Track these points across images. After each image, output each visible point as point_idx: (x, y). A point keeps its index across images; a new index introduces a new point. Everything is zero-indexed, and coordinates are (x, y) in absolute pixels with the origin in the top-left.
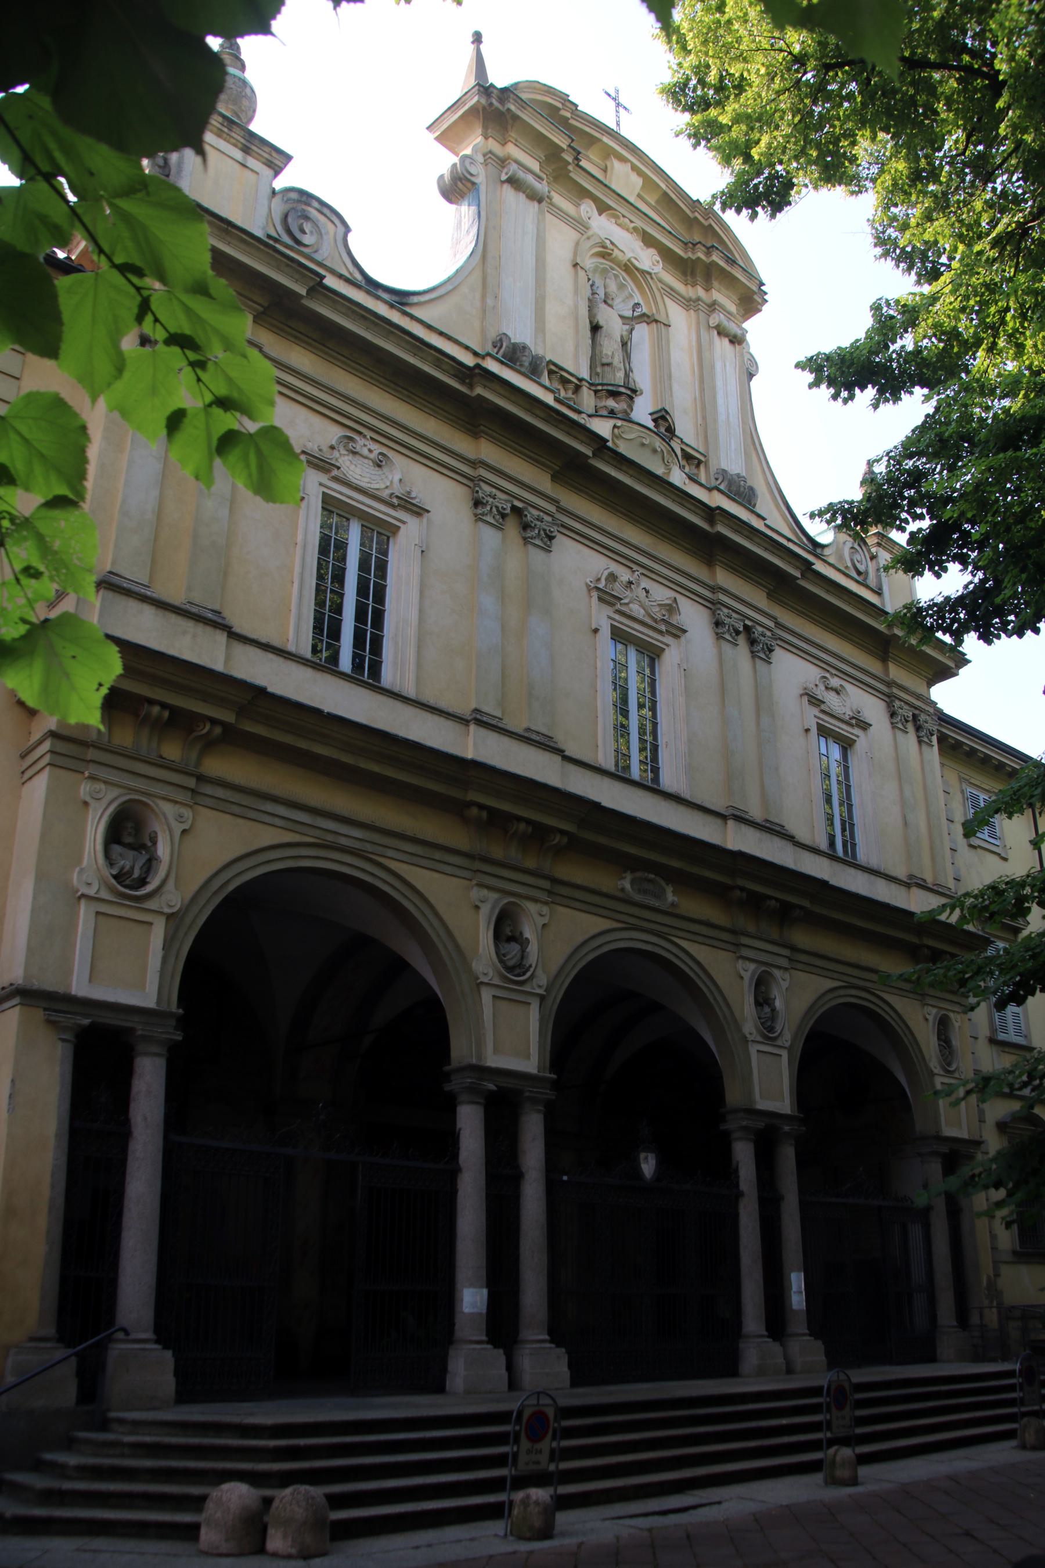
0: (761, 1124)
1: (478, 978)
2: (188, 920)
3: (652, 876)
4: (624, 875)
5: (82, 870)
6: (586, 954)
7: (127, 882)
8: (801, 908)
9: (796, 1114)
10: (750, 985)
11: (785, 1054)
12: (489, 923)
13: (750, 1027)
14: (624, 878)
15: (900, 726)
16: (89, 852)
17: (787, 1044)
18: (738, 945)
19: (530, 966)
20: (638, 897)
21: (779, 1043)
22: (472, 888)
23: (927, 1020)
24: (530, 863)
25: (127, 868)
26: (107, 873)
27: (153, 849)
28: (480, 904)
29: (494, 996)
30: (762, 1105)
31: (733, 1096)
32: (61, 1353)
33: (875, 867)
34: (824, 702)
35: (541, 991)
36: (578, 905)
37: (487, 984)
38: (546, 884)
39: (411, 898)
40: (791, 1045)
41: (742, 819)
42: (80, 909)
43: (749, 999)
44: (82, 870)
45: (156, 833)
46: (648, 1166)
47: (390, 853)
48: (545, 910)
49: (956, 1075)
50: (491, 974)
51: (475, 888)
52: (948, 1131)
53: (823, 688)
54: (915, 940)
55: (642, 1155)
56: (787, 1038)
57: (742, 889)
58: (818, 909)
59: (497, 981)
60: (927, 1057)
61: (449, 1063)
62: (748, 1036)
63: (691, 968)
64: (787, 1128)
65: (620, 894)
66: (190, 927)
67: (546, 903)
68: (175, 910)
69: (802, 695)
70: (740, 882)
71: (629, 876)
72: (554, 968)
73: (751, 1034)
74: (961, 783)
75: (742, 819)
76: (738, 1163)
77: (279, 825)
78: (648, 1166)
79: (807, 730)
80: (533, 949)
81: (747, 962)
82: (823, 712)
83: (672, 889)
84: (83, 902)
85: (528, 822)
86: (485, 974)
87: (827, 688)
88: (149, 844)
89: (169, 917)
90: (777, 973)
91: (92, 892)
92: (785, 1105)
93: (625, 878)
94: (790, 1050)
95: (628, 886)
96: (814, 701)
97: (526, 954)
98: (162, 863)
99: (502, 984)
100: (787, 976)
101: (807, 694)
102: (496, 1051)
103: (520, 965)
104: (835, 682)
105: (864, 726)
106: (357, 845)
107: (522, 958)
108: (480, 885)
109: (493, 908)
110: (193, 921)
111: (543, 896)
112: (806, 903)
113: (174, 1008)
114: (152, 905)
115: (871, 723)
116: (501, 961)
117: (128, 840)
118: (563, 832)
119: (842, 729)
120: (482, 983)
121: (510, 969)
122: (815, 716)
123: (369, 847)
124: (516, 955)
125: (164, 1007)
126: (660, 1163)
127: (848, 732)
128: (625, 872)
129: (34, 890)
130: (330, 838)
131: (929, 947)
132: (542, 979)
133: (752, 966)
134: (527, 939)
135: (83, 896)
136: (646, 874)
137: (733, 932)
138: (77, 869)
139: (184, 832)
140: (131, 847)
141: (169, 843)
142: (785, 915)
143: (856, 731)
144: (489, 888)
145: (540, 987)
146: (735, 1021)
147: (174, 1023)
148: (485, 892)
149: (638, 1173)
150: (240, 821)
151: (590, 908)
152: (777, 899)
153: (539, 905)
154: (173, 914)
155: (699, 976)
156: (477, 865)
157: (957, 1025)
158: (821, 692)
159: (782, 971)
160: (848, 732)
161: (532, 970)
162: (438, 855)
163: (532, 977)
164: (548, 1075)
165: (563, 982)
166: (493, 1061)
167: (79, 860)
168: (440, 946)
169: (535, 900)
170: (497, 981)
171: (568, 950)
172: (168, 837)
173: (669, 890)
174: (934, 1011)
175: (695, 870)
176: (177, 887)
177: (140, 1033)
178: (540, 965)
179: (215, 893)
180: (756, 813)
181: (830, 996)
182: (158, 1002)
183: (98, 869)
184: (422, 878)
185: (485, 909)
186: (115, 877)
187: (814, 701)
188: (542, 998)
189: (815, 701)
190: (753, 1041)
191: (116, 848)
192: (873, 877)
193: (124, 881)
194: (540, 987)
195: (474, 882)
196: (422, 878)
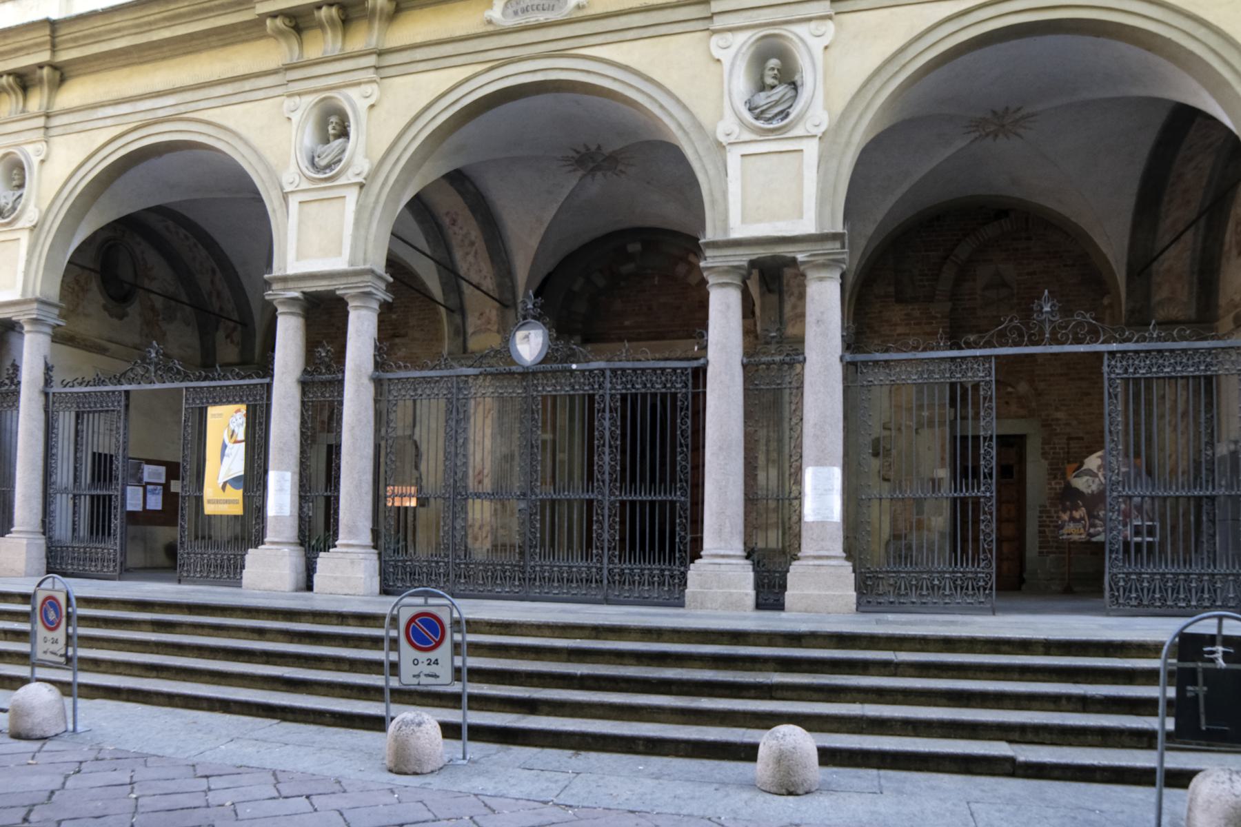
2: (46, 227)
18: (710, 18)
28: (291, 115)
35: (360, 179)
37: (292, 192)
38: (372, 60)
59: (305, 185)
63: (615, 79)
65: (490, 28)
66: (49, 231)
77: (110, 124)
81: (729, 35)
102: (300, 256)
108: (290, 95)
110: (51, 227)
111: (370, 74)
114: (19, 225)
123: (182, 109)
130: (150, 116)
139: (43, 161)
146: (700, 127)
148: (297, 99)
150: (82, 135)
151: (438, 64)
154: (35, 226)
159: (813, 24)
162: (247, 85)
165: (398, 159)
170: (305, 185)
179: (66, 199)
184: (233, 116)
190: (730, 144)
194: (358, 174)
196: (233, 116)
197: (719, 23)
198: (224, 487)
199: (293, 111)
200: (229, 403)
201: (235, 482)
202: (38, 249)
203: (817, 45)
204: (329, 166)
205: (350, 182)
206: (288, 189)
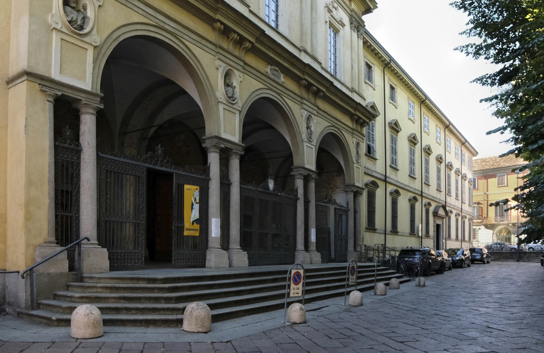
0: (306, 173)
1: (218, 100)
2: (103, 51)
3: (277, 69)
4: (268, 66)
5: (53, 15)
6: (254, 97)
7: (75, 26)
8: (323, 92)
9: (316, 171)
10: (305, 119)
11: (314, 147)
12: (222, 78)
13: (304, 136)
14: (267, 68)
15: (353, 28)
16: (56, 6)
17: (315, 144)
19: (237, 98)
20: (272, 77)
21: (312, 143)
22: (216, 60)
23: (353, 143)
24: (237, 53)
25: (74, 19)
26: (65, 19)
27: (85, 12)
28: (219, 68)
29: (224, 108)
30: (307, 166)
31: (296, 162)
32: (59, 249)
33: (343, 82)
34: (332, 12)
35: (240, 109)
36: (252, 75)
37: (222, 103)
38: (242, 64)
39: (193, 59)
40: (316, 145)
41: (306, 52)
42: (53, 36)
43: (305, 125)
44: (53, 15)
45: (87, 5)
46: (271, 185)
47: (185, 37)
48: (241, 75)
49: (360, 164)
50: (223, 98)
51: (217, 61)
52: (357, 184)
53: (332, 6)
54: (353, 112)
55: (270, 181)
56: (314, 142)
57: (306, 80)
58: (327, 94)
59: (225, 102)
60: (352, 156)
61: (205, 135)
62: (304, 139)
64: (313, 176)
65: (266, 74)
67: (241, 72)
68: (97, 44)
69: (325, 7)
70: (306, 77)
71: (269, 67)
72: (244, 100)
73: (305, 138)
74: (364, 58)
75: (306, 52)
76: (297, 187)
78: (271, 185)
79: (326, 22)
80: (237, 90)
82: (331, 16)
83: (283, 76)
84: (54, 32)
85: (239, 34)
86: (221, 98)
87: (333, 6)
88: (83, 10)
89: (95, 47)
90: (313, 116)
91: (59, 27)
92: (313, 168)
93: (268, 67)
94: (315, 146)
95: (269, 71)
96: (330, 11)
97: (234, 92)
98: (91, 20)
99: (226, 103)
100: (316, 118)
101: (327, 7)
102: (225, 131)
103: (232, 97)
104: (336, 5)
105: (343, 25)
106: (173, 30)
107: (233, 94)
108: (219, 59)
109: (223, 70)
112: (324, 90)
113: (99, 92)
114: (87, 39)
115: (346, 24)
116: (227, 94)
117: (74, 5)
118: (250, 42)
119: (336, 25)
120: (219, 102)
121: (229, 98)
122: (329, 17)
124: (231, 92)
125: (94, 91)
126: (275, 184)
127: (338, 26)
128: (268, 65)
129: (29, 21)
130: (162, 24)
131: (357, 116)
132: (240, 104)
133: (306, 112)
134: (235, 86)
135: (54, 28)
136: (275, 68)
137: (301, 98)
138: (50, 15)
140: (73, 8)
141: (94, 10)
142: (317, 94)
143: (341, 27)
144: (221, 61)
145: (239, 107)
146: (300, 133)
147: (99, 99)
148: (221, 63)
149: (268, 188)
151: (257, 78)
152: (317, 87)
153: (240, 73)
155: (289, 113)
156: (219, 50)
157: (361, 146)
158: (331, 7)
160: (338, 26)
161: (237, 99)
162: (204, 42)
163: (236, 103)
164: (241, 144)
165: (246, 108)
166: (224, 136)
167: (50, 10)
168: (204, 83)
169: (238, 70)
171: (249, 94)
172: (93, 7)
173: (282, 76)
174: (355, 140)
175: (291, 69)
176: (98, 33)
177: (85, 102)
178: (239, 98)
179: (114, 40)
180: (309, 50)
181: (327, 129)
182: (92, 89)
183: (61, 17)
185: (221, 70)
186: (70, 22)
187: (330, 11)
188: (240, 112)
189: (330, 11)
190: (305, 141)
191: (68, 8)
192: (342, 86)
193: (73, 25)
194: (239, 107)
195: (217, 57)
197: (305, 106)
198: (193, 223)
199: (220, 67)
200: (194, 185)
201: (196, 221)
202: (98, 62)
203: (315, 121)
204: (229, 98)
205: (237, 108)
206: (220, 100)
